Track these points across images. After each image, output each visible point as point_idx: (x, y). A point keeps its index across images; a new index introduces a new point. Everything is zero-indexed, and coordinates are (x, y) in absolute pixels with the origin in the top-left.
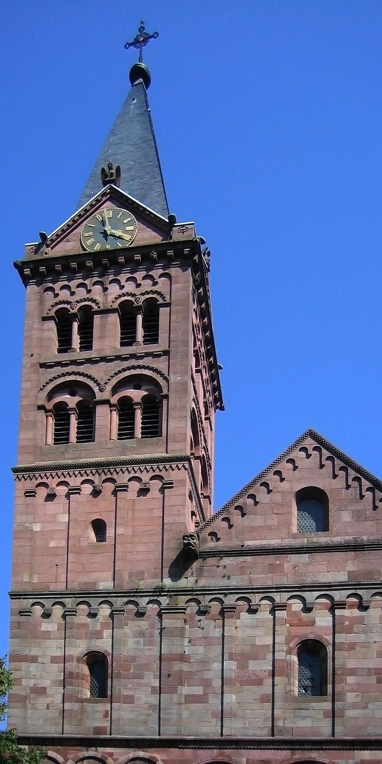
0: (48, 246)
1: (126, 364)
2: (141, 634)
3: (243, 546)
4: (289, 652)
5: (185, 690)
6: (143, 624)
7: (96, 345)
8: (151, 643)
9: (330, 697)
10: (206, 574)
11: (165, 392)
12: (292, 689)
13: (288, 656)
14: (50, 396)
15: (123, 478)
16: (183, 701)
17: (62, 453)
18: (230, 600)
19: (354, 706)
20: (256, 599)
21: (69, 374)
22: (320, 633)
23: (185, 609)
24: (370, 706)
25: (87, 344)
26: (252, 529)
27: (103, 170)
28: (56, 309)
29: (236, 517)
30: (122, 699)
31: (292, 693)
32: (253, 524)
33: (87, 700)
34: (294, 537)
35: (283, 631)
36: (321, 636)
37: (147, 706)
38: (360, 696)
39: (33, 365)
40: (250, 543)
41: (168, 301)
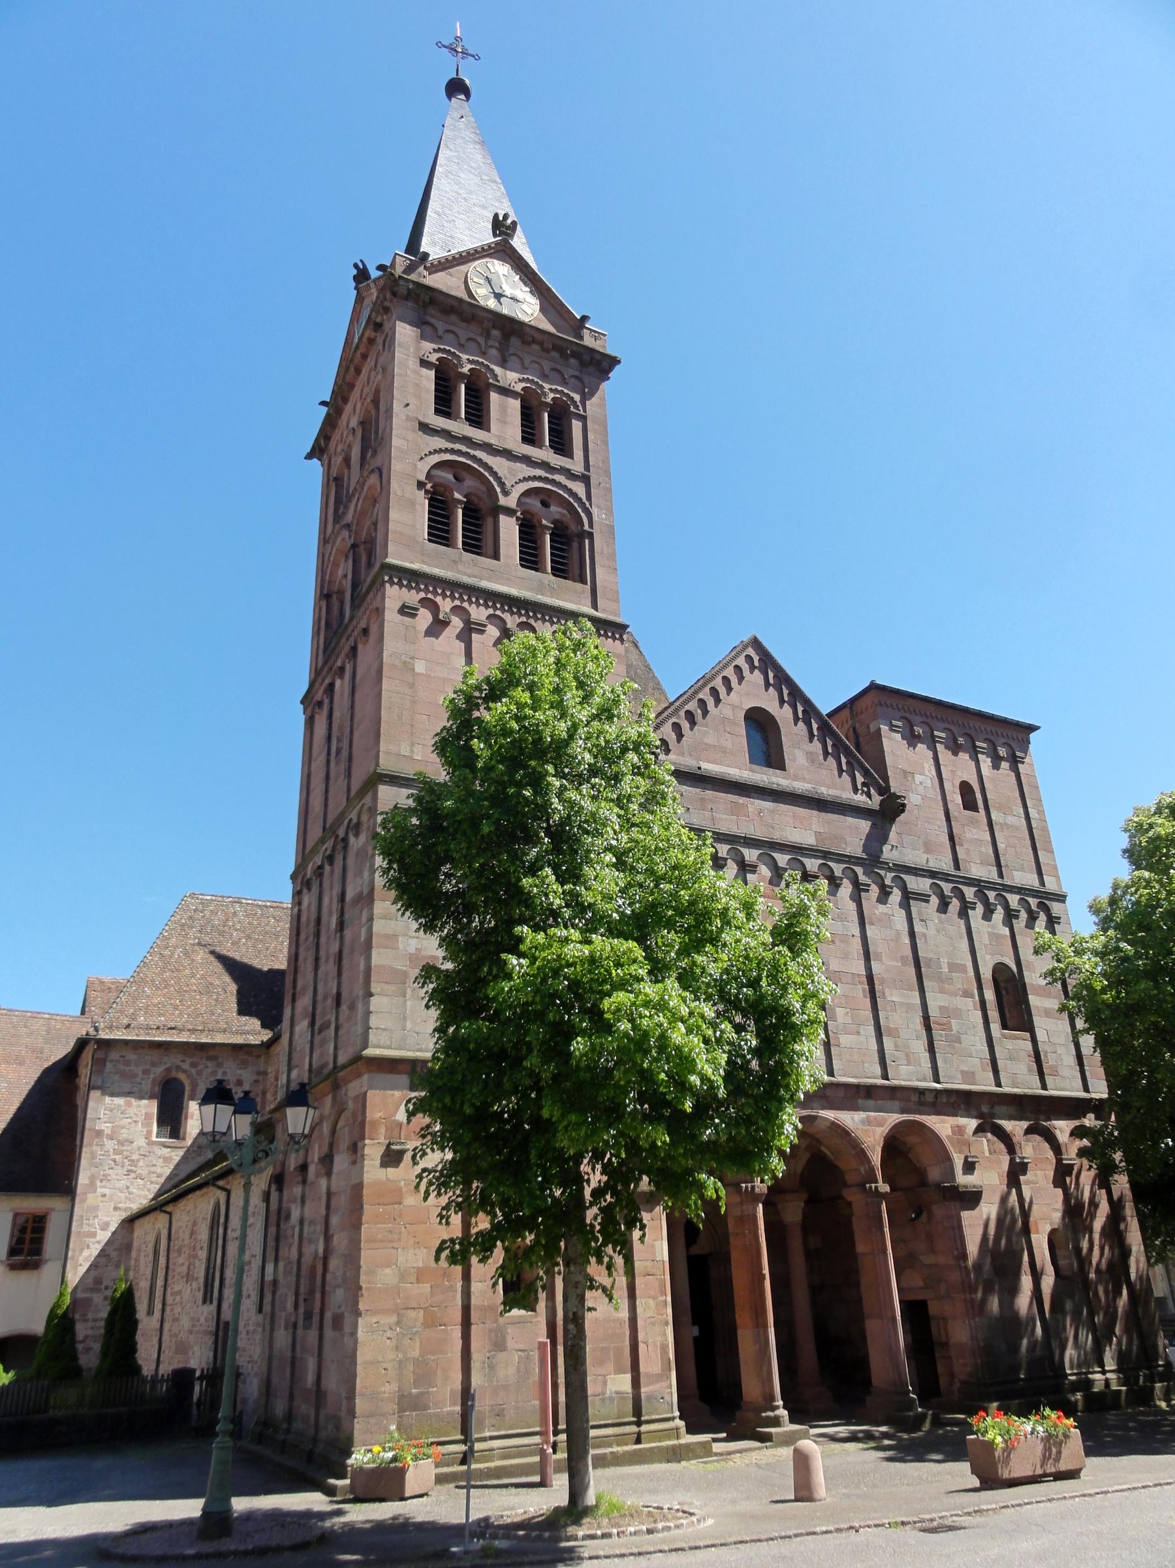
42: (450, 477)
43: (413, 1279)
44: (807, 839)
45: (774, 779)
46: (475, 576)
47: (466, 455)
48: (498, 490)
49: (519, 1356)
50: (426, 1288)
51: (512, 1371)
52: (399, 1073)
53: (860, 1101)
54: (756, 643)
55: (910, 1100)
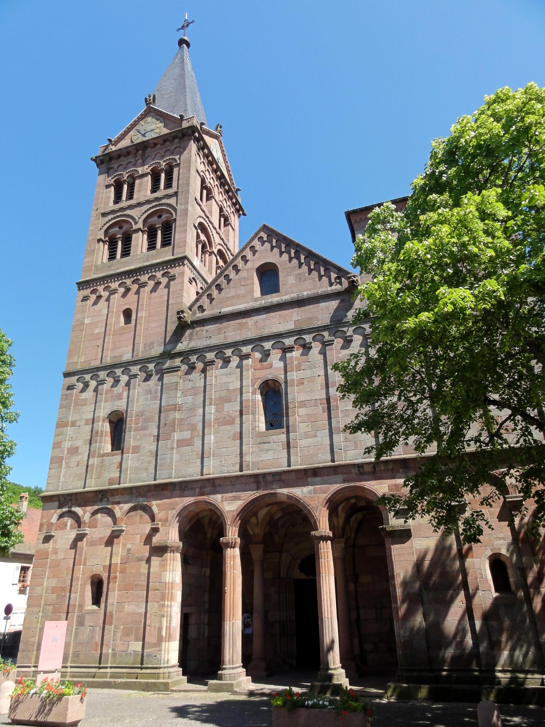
0: (112, 145)
2: (149, 392)
3: (220, 313)
4: (254, 393)
5: (176, 436)
7: (135, 196)
8: (155, 398)
9: (284, 430)
10: (195, 337)
11: (174, 217)
12: (257, 425)
13: (254, 396)
14: (106, 232)
15: (144, 278)
16: (175, 446)
17: (110, 267)
18: (210, 356)
19: (306, 435)
20: (228, 352)
21: (118, 217)
22: (276, 373)
23: (180, 367)
24: (318, 434)
25: (130, 196)
26: (228, 299)
27: (146, 99)
28: (114, 179)
29: (215, 293)
30: (131, 450)
31: (257, 429)
32: (228, 296)
33: (107, 455)
34: (256, 300)
35: (249, 375)
36: (277, 376)
37: (149, 453)
38: (310, 426)
40: (226, 310)
42: (117, 229)
43: (50, 592)
44: (290, 326)
45: (270, 300)
46: (117, 269)
47: (121, 216)
48: (133, 223)
49: (90, 629)
50: (54, 596)
51: (85, 636)
52: (54, 501)
53: (309, 479)
54: (265, 228)
55: (351, 473)
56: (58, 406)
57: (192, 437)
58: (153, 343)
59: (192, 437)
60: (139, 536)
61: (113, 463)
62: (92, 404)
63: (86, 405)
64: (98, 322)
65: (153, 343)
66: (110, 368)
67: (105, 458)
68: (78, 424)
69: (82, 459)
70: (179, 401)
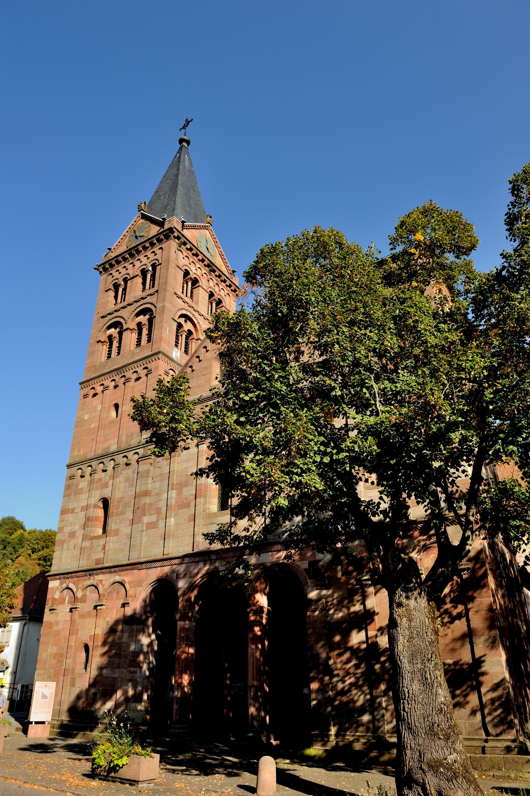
1: (139, 303)
5: (146, 520)
6: (129, 471)
11: (154, 315)
16: (145, 528)
37: (125, 536)
39: (98, 319)
41: (160, 262)
43: (52, 657)
56: (62, 495)
57: (158, 520)
58: (133, 434)
59: (158, 520)
60: (115, 610)
61: (100, 545)
62: (86, 492)
63: (82, 493)
64: (94, 417)
65: (133, 434)
66: (101, 458)
67: (94, 540)
68: (76, 511)
69: (78, 542)
70: (150, 487)
